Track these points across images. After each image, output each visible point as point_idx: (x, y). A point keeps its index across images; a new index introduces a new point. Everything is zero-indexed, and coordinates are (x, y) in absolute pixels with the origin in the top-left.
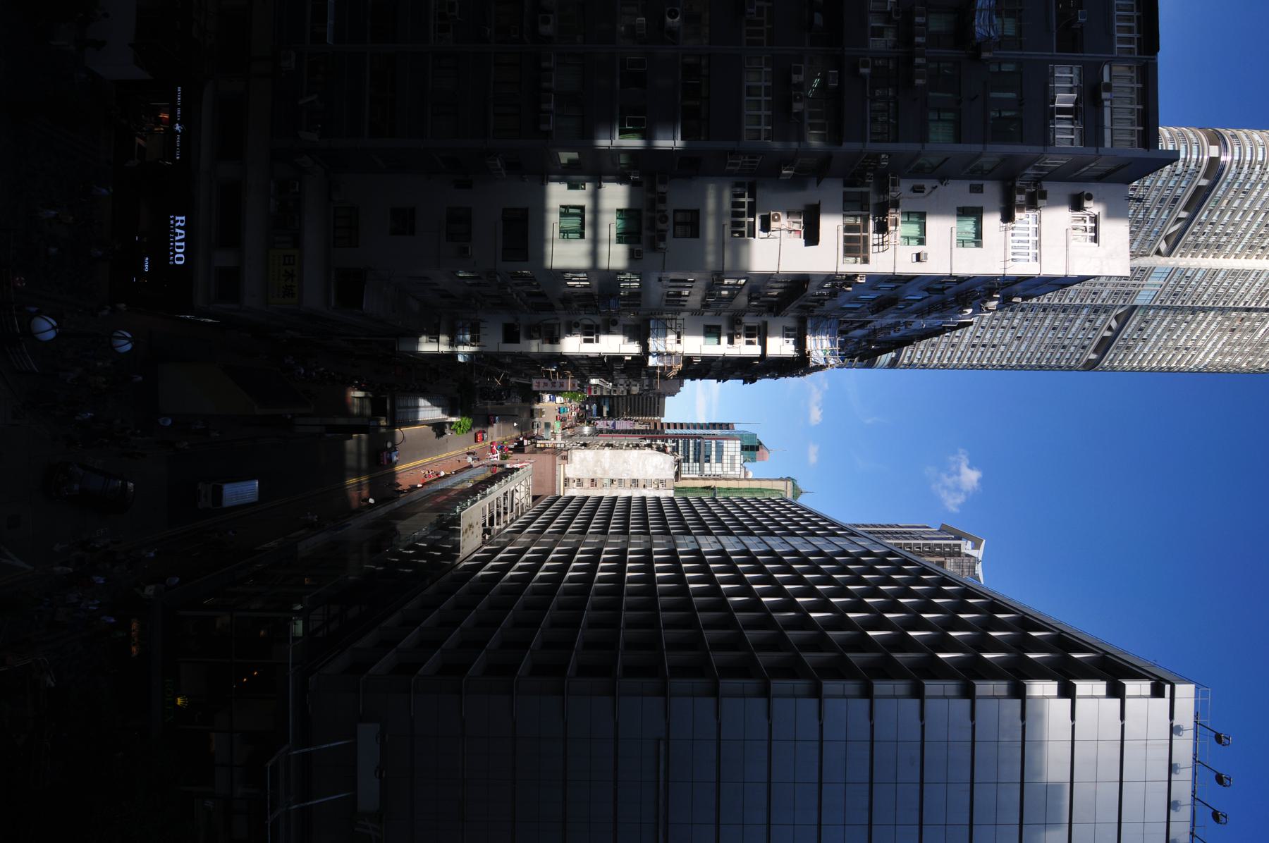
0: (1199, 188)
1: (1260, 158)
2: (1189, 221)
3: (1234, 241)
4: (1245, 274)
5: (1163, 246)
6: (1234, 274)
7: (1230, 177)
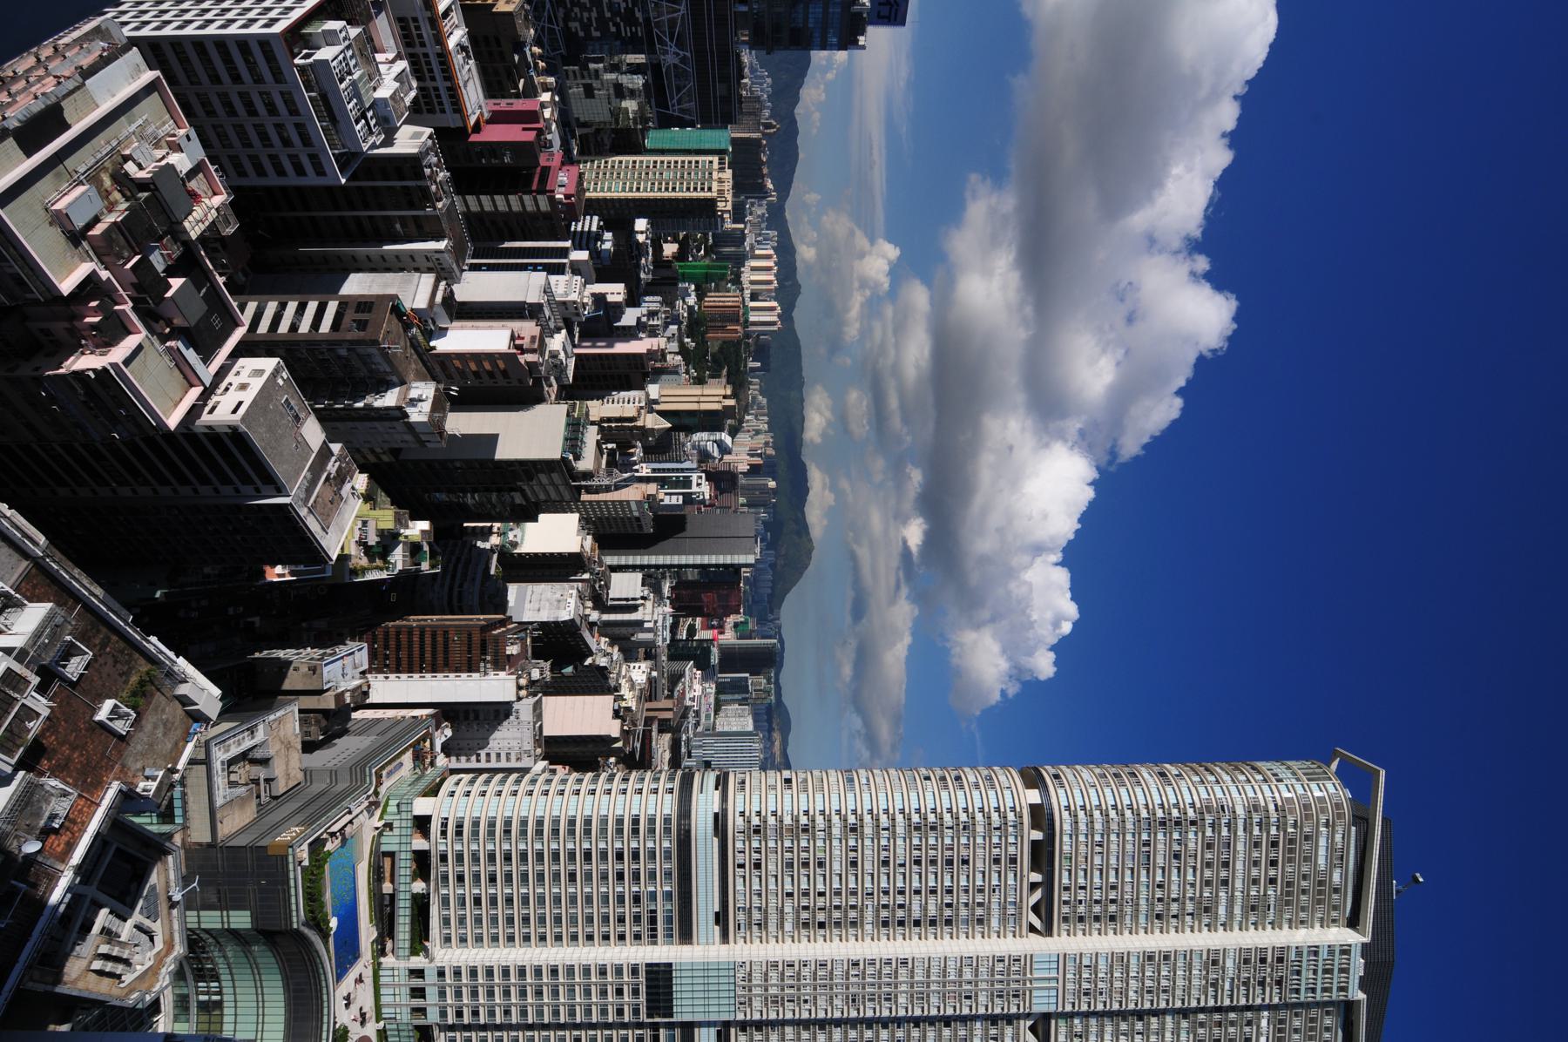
0: (1034, 844)
1: (1142, 801)
2: (1048, 885)
3: (1128, 910)
4: (1166, 958)
5: (1037, 923)
6: (1151, 958)
7: (1067, 827)
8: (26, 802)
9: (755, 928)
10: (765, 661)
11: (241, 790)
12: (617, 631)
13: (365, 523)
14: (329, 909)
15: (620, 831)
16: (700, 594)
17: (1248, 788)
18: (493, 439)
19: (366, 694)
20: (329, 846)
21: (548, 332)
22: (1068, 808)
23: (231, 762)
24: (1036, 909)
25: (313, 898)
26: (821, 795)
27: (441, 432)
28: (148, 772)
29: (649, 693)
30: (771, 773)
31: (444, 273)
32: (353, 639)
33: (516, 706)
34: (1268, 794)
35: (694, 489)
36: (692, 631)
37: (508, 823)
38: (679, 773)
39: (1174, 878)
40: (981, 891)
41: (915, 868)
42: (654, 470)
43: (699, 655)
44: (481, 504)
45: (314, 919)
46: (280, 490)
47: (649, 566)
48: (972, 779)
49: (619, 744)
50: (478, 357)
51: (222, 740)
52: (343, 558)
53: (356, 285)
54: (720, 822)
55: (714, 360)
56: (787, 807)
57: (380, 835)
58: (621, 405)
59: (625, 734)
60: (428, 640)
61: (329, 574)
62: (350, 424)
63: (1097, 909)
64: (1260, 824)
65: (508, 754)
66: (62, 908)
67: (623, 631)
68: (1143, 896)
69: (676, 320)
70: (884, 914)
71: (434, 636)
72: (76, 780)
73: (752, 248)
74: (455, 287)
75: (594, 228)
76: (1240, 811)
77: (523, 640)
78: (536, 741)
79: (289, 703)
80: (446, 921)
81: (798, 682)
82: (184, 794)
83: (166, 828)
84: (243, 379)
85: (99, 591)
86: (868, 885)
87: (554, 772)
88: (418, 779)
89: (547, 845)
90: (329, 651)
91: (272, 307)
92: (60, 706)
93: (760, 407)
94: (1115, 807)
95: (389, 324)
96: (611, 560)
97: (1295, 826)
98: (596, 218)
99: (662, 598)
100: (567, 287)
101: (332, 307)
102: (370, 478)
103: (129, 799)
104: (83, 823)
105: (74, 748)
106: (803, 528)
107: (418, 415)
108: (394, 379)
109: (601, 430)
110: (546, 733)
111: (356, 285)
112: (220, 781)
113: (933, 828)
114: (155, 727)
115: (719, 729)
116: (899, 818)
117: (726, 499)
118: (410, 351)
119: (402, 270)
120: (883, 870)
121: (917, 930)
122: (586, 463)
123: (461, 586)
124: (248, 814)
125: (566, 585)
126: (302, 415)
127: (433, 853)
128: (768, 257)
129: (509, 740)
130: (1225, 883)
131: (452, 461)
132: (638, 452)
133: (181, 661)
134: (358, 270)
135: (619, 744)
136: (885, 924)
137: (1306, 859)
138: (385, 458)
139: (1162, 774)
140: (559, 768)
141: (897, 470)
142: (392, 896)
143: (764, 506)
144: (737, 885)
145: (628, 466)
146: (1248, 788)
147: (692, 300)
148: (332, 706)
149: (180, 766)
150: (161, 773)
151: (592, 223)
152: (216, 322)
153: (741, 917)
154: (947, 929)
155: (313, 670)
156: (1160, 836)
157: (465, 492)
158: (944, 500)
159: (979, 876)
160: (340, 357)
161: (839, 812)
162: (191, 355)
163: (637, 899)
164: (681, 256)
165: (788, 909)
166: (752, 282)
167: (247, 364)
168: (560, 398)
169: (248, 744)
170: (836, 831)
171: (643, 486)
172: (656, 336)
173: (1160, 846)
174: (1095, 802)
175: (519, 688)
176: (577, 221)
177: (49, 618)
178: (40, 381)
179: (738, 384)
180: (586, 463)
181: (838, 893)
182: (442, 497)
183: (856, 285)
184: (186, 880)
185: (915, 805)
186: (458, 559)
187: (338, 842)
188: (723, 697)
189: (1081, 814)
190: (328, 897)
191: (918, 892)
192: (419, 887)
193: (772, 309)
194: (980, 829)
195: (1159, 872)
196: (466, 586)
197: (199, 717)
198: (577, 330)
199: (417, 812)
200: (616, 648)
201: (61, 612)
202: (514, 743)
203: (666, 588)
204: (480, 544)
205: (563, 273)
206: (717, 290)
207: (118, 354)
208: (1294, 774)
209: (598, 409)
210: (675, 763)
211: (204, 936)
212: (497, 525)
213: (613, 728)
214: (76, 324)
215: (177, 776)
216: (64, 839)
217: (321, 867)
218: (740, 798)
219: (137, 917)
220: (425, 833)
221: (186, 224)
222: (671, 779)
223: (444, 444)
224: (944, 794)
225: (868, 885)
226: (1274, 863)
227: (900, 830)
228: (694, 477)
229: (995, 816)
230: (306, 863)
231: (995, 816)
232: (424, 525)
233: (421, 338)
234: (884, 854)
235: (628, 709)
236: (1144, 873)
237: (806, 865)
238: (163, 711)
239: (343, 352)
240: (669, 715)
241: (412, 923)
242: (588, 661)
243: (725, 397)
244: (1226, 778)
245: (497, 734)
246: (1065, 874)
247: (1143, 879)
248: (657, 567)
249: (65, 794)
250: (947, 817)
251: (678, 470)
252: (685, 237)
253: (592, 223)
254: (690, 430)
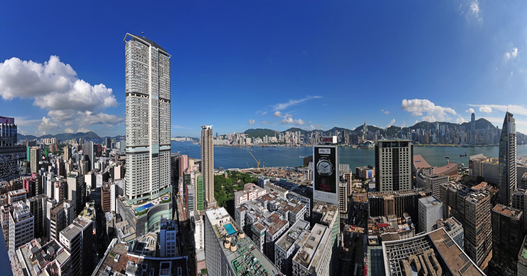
8: (130, 270)
16: (98, 152)
18: (73, 191)
21: (56, 181)
23: (124, 234)
26: (130, 130)
29: (114, 160)
36: (104, 153)
50: (60, 194)
52: (92, 219)
53: (48, 217)
54: (133, 147)
59: (120, 164)
95: (54, 210)
101: (52, 221)
103: (129, 251)
106: (87, 133)
111: (48, 217)
112: (127, 235)
117: (83, 147)
122: (76, 173)
129: (121, 185)
132: (75, 164)
133: (109, 248)
144: (142, 144)
145: (77, 166)
147: (51, 154)
149: (124, 243)
152: (54, 245)
162: (59, 250)
167: (60, 239)
168: (66, 179)
169: (121, 232)
179: (64, 145)
180: (76, 173)
197: (117, 242)
203: (97, 158)
209: (68, 172)
210: (124, 155)
213: (119, 166)
232: (87, 204)
254: (71, 154)
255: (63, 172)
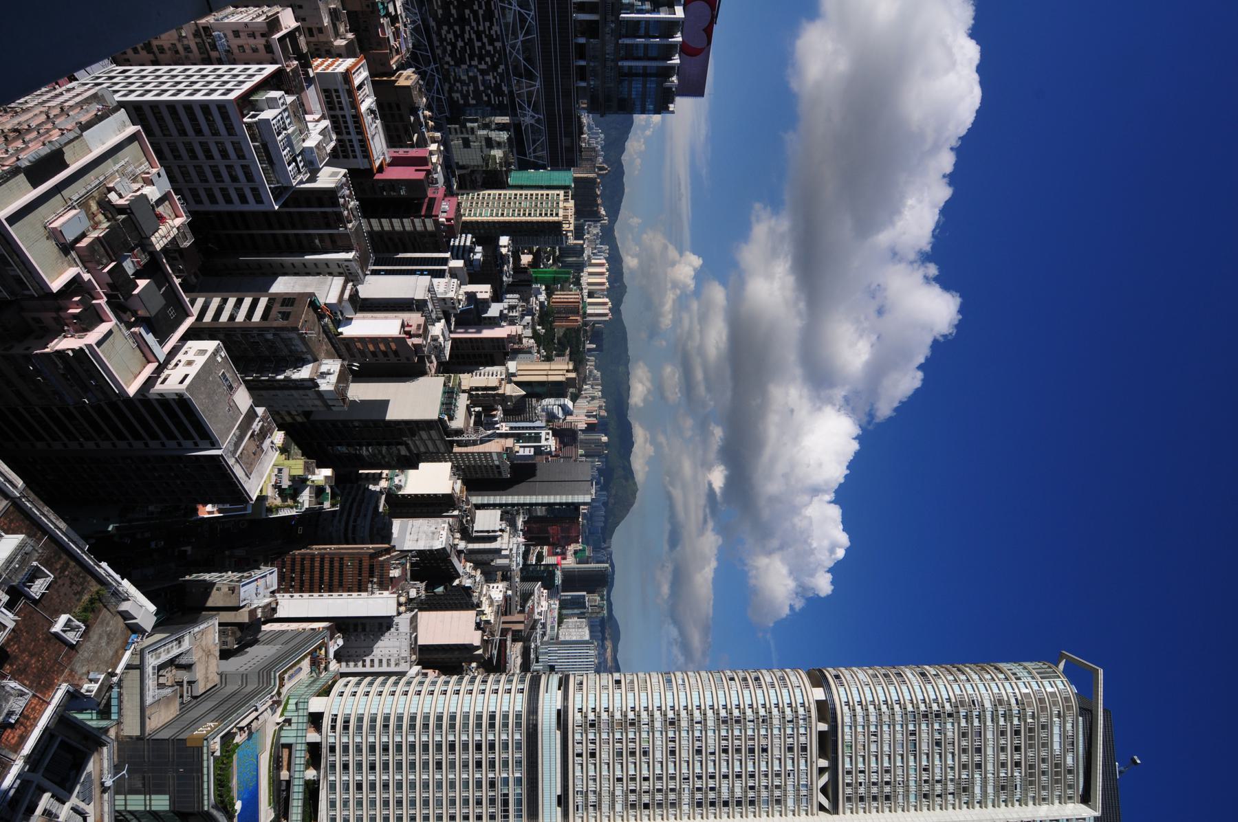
0: (821, 734)
3: (900, 790)
5: (825, 803)
7: (847, 720)
9: (591, 809)
10: (599, 582)
11: (168, 691)
12: (479, 557)
13: (280, 470)
14: (235, 793)
15: (479, 726)
16: (547, 527)
17: (993, 685)
18: (385, 404)
19: (274, 610)
20: (238, 739)
21: (430, 321)
22: (847, 703)
23: (161, 667)
24: (824, 790)
25: (222, 783)
26: (645, 694)
27: (344, 398)
28: (92, 676)
29: (505, 608)
30: (604, 675)
31: (351, 276)
32: (266, 565)
33: (396, 620)
34: (1010, 690)
35: (543, 443)
36: (540, 557)
37: (387, 718)
38: (529, 675)
39: (937, 762)
40: (778, 775)
41: (723, 755)
42: (511, 428)
43: (544, 576)
44: (374, 455)
45: (222, 802)
46: (214, 444)
47: (506, 505)
48: (768, 679)
49: (480, 652)
51: (154, 648)
52: (262, 498)
53: (283, 285)
54: (562, 716)
55: (560, 342)
56: (618, 705)
57: (281, 729)
58: (487, 377)
59: (485, 643)
60: (327, 565)
61: (249, 511)
62: (273, 392)
63: (874, 790)
64: (1004, 716)
65: (389, 660)
66: (12, 792)
67: (485, 557)
68: (912, 778)
69: (530, 312)
70: (698, 796)
71: (332, 562)
72: (32, 682)
73: (589, 258)
74: (359, 287)
75: (468, 243)
76: (988, 705)
77: (403, 565)
78: (412, 649)
79: (211, 617)
80: (332, 804)
81: (626, 598)
82: (120, 694)
83: (103, 723)
84: (190, 357)
85: (63, 525)
86: (684, 771)
87: (426, 675)
88: (314, 682)
89: (419, 738)
90: (246, 574)
91: (216, 302)
92: (24, 619)
93: (595, 379)
94: (886, 702)
95: (306, 315)
96: (476, 500)
97: (1033, 717)
98: (470, 236)
99: (516, 530)
100: (446, 288)
101: (263, 302)
102: (286, 435)
103: (75, 699)
104: (35, 719)
105: (32, 655)
106: (629, 473)
107: (326, 385)
108: (309, 357)
109: (471, 397)
110: (420, 642)
111: (283, 285)
112: (151, 683)
113: (738, 722)
114: (100, 637)
115: (562, 638)
116: (710, 713)
117: (568, 450)
118: (323, 336)
119: (318, 274)
120: (697, 758)
121: (726, 809)
122: (458, 423)
123: (355, 521)
124: (173, 711)
125: (439, 520)
126: (235, 385)
127: (324, 745)
128: (601, 265)
129: (390, 648)
130: (979, 766)
131: (352, 421)
132: (499, 413)
133: (126, 583)
134: (285, 274)
135: (480, 652)
136: (699, 805)
137: (1044, 745)
138: (299, 419)
139: (923, 674)
140: (430, 672)
141: (703, 427)
142: (288, 782)
143: (599, 456)
144: (576, 772)
145: (491, 425)
146: (993, 685)
147: (542, 297)
148: (247, 620)
149: (118, 671)
150: (102, 677)
151: (467, 240)
152: (172, 313)
153: (579, 799)
154: (750, 809)
155: (232, 590)
156: (924, 727)
157: (361, 445)
158: (741, 450)
159: (776, 762)
160: (267, 340)
161: (660, 708)
162: (150, 339)
163: (492, 784)
164: (534, 264)
165: (618, 792)
166: (589, 284)
167: (193, 345)
168: (438, 372)
169: (175, 651)
170: (658, 725)
171: (502, 441)
172: (514, 324)
173: (924, 735)
174: (869, 698)
175: (399, 604)
176: (455, 238)
177: (21, 546)
178: (29, 358)
179: (578, 361)
180: (458, 423)
181: (660, 778)
182: (343, 449)
183: (669, 286)
184: (117, 768)
185: (722, 702)
186: (354, 499)
187: (245, 735)
188: (564, 612)
189: (858, 708)
190: (235, 781)
191: (726, 777)
192: (311, 774)
193: (605, 304)
194: (776, 722)
195: (924, 757)
196: (359, 522)
197: (137, 630)
198: (453, 319)
199: (311, 710)
200: (479, 572)
201: (31, 542)
202: (394, 651)
204: (371, 487)
205: (443, 277)
206: (562, 289)
207: (93, 337)
208: (1030, 673)
209: (468, 380)
210: (525, 667)
211: (129, 817)
212: (385, 472)
213: (475, 638)
214: (62, 314)
215: (115, 679)
216: (18, 732)
217: (230, 757)
218: (578, 696)
219: (74, 800)
220: (318, 728)
221: (153, 239)
222: (522, 681)
223: (346, 408)
224: (746, 692)
225: (684, 771)
226: (1018, 749)
227: (710, 723)
228: (543, 433)
229: (788, 711)
230: (218, 754)
231: (788, 711)
232: (328, 472)
233: (331, 326)
234: (697, 744)
235: (488, 622)
236: (912, 758)
237: (633, 754)
238: (108, 624)
239: (270, 336)
240: (521, 627)
241: (304, 806)
242: (456, 582)
243: (568, 371)
244: (975, 677)
245: (380, 643)
246: (847, 760)
247: (912, 763)
248: (513, 505)
249: (22, 694)
250: (749, 712)
251: (530, 428)
252: (538, 250)
253: (467, 240)
254: (540, 397)
255: (469, 356)
